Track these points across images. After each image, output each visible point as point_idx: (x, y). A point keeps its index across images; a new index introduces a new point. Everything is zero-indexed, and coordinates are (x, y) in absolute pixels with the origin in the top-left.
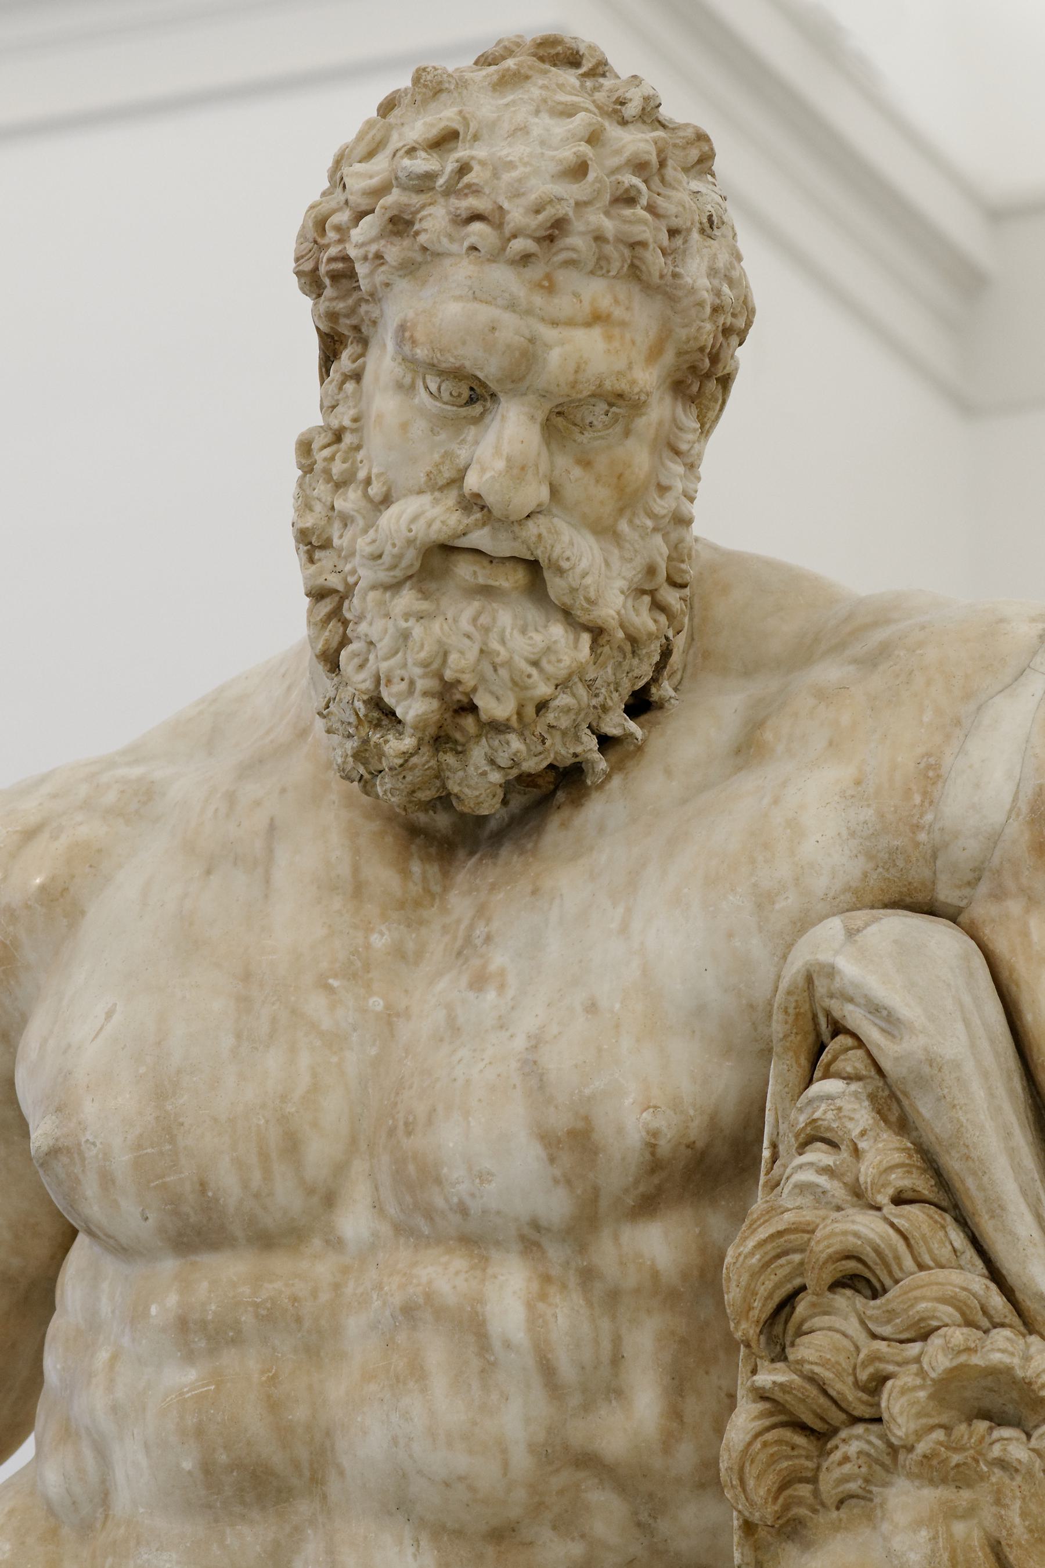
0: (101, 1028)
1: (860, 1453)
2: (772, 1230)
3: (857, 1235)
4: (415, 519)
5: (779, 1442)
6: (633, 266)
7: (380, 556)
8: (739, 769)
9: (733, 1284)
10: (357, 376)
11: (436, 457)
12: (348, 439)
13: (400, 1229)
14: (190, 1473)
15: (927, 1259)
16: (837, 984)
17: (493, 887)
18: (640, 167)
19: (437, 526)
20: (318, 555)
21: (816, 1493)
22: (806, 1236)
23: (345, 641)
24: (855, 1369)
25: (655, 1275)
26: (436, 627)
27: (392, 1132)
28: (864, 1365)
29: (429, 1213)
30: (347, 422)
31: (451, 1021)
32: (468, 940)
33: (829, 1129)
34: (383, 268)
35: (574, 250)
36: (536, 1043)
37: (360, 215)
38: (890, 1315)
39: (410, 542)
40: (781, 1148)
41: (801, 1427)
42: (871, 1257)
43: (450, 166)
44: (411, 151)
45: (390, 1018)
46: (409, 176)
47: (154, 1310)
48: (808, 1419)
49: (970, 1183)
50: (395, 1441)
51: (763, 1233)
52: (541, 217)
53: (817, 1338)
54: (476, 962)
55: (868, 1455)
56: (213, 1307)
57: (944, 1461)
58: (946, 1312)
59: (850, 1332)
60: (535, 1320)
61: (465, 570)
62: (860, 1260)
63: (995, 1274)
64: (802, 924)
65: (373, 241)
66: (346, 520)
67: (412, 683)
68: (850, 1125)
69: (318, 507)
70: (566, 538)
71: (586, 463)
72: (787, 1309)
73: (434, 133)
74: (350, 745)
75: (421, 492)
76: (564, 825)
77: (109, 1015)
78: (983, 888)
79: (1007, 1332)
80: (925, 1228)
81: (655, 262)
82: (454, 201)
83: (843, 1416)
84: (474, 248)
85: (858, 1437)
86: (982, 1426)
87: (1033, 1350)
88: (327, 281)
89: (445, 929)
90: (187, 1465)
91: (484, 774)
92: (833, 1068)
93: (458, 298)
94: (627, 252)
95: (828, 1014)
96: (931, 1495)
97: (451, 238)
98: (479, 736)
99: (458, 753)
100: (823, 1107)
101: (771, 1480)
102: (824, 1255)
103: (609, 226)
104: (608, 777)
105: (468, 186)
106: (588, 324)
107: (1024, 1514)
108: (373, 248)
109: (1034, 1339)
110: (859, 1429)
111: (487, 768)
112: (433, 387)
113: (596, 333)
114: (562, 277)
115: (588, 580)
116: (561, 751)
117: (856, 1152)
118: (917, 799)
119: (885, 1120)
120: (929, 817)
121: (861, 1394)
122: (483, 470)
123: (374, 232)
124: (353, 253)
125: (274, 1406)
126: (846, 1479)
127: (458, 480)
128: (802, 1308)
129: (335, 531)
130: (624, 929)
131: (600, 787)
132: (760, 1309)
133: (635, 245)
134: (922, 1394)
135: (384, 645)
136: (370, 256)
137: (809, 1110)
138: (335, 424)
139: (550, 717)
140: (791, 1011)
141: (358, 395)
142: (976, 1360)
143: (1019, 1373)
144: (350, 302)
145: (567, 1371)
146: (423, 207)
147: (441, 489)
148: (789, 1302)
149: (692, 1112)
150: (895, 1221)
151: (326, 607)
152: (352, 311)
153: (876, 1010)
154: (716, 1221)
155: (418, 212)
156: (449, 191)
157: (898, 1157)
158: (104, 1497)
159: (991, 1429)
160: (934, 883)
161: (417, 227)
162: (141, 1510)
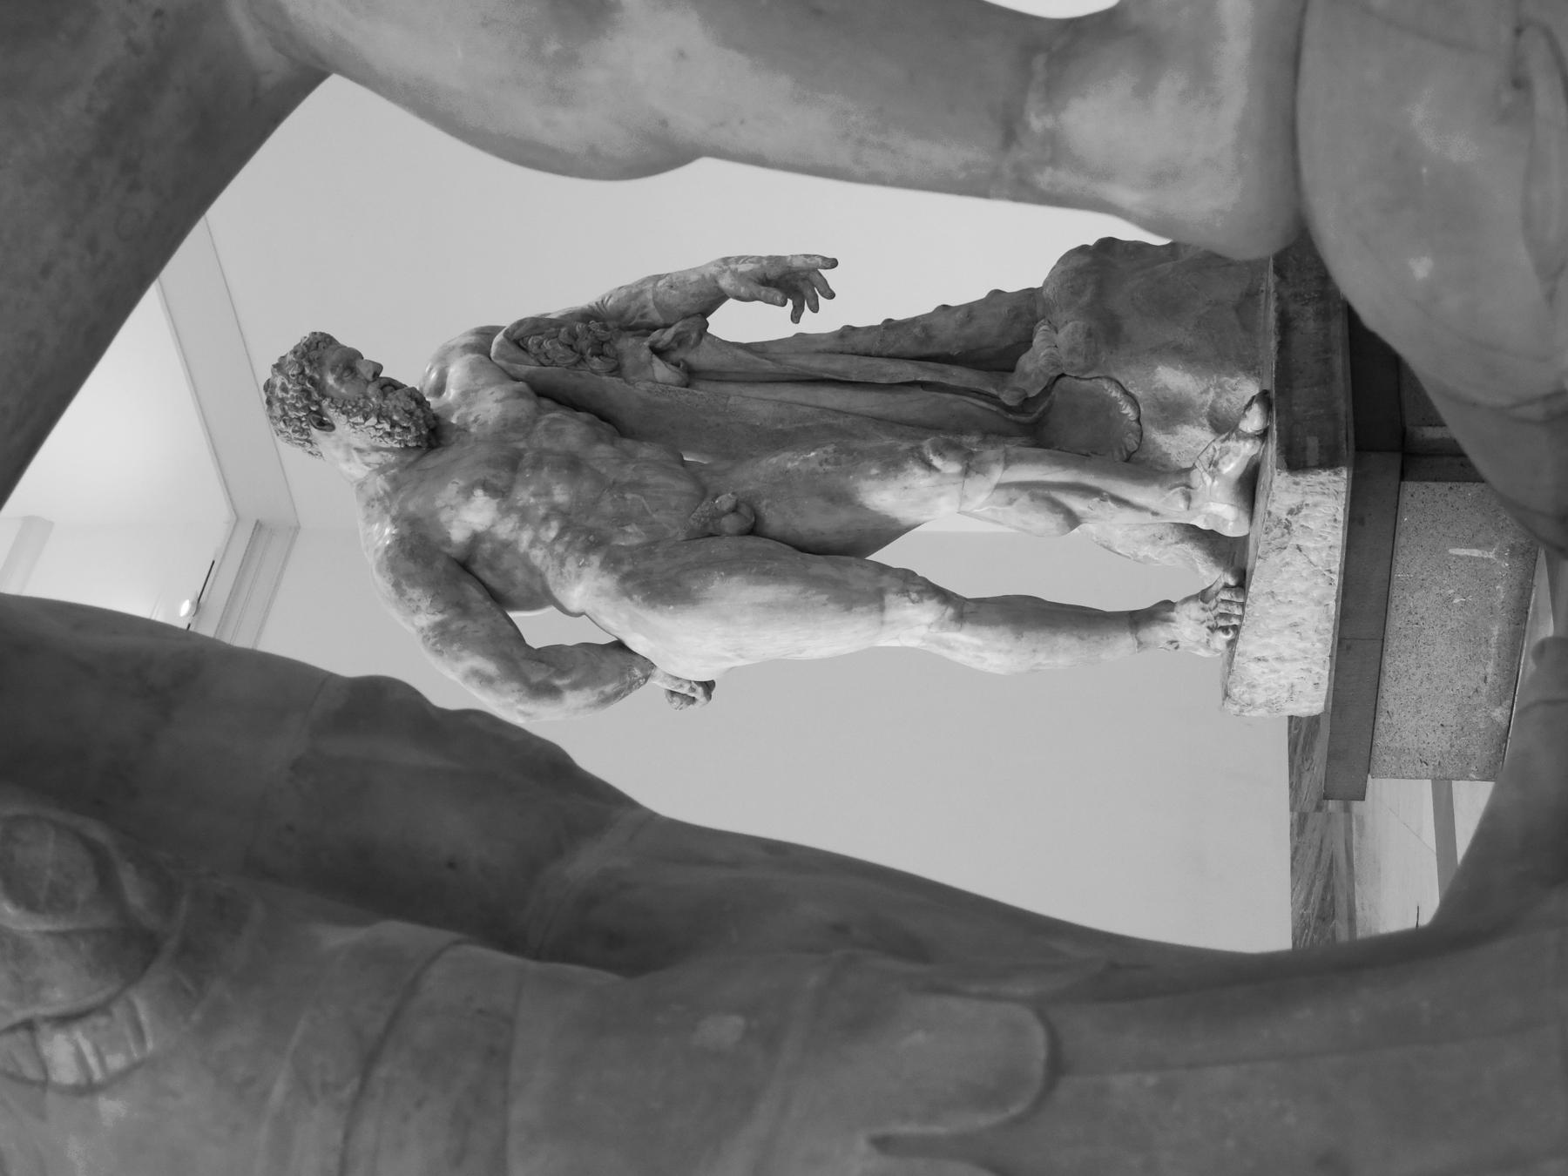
13: (527, 436)
16: (510, 331)
23: (391, 418)
36: (497, 401)
37: (302, 372)
45: (476, 440)
74: (413, 429)
82: (312, 348)
84: (324, 348)
90: (566, 472)
127: (368, 382)
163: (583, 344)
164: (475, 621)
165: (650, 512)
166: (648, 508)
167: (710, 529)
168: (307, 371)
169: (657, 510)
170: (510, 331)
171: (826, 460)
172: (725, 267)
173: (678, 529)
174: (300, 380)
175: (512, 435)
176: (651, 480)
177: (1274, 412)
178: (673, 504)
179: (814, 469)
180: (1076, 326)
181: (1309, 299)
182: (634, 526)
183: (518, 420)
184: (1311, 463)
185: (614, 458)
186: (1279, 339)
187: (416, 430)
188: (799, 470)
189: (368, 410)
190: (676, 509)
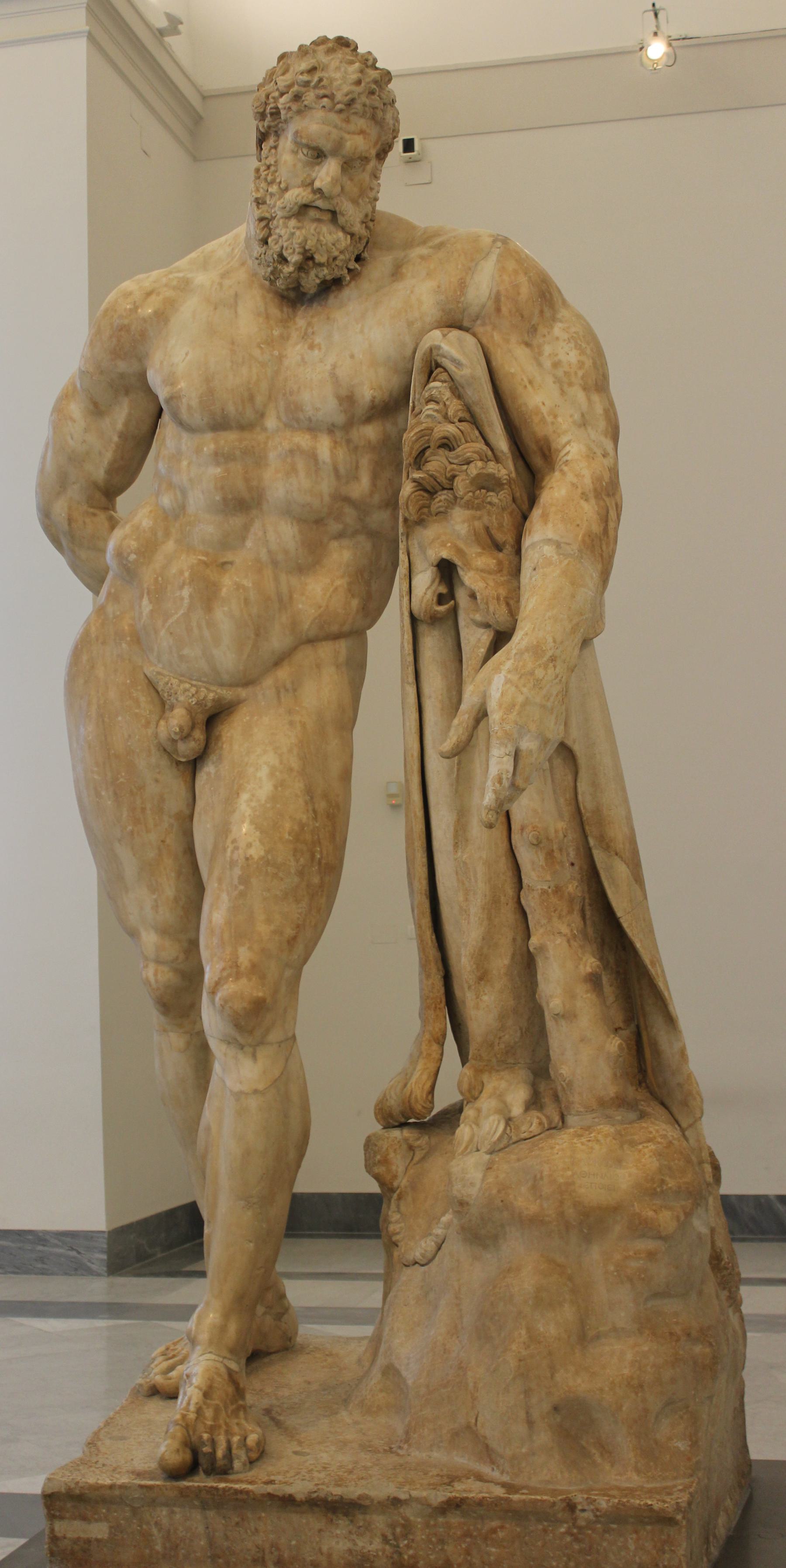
0: (185, 358)
1: (445, 499)
2: (419, 429)
3: (448, 431)
4: (298, 196)
5: (420, 495)
6: (373, 115)
7: (285, 208)
8: (394, 281)
9: (406, 446)
10: (275, 147)
11: (305, 175)
12: (272, 168)
13: (286, 425)
14: (218, 501)
15: (469, 439)
16: (441, 351)
17: (312, 317)
18: (376, 82)
19: (305, 198)
20: (260, 206)
21: (430, 512)
22: (430, 431)
23: (270, 235)
24: (445, 473)
25: (369, 442)
26: (304, 231)
27: (284, 395)
28: (449, 472)
29: (298, 420)
30: (272, 163)
31: (303, 359)
32: (306, 334)
33: (436, 397)
34: (291, 112)
35: (356, 109)
36: (334, 367)
37: (282, 95)
38: (458, 457)
39: (296, 203)
40: (416, 403)
41: (426, 490)
42: (452, 439)
43: (316, 79)
44: (302, 73)
45: (280, 358)
46: (302, 81)
47: (205, 449)
48: (429, 488)
49: (483, 416)
50: (287, 492)
51: (417, 430)
52: (348, 98)
53: (433, 463)
54: (310, 341)
55: (448, 500)
56: (226, 449)
57: (473, 502)
58: (476, 456)
59: (443, 462)
60: (333, 455)
61: (312, 213)
62: (449, 440)
63: (487, 443)
64: (423, 332)
65: (288, 103)
66: (272, 195)
67: (294, 250)
68: (443, 396)
69: (261, 191)
70: (345, 204)
71: (351, 180)
72: (421, 454)
73: (309, 67)
74: (269, 270)
75: (299, 187)
76: (336, 297)
77: (187, 354)
78: (479, 322)
79: (493, 463)
80: (469, 430)
81: (380, 114)
83: (441, 488)
84: (324, 107)
85: (445, 494)
86: (483, 491)
87: (500, 468)
88: (269, 116)
89: (297, 329)
90: (218, 498)
91: (314, 280)
92: (437, 378)
93: (317, 123)
94: (372, 110)
95: (436, 361)
96: (468, 513)
97: (316, 103)
98: (313, 268)
99: (305, 273)
100: (434, 391)
101: (417, 507)
102: (438, 438)
103: (368, 102)
104: (350, 282)
105: (323, 86)
106: (359, 134)
107: (496, 519)
108: (288, 105)
109: (500, 464)
110: (445, 492)
111: (315, 278)
112: (305, 152)
113: (361, 137)
114: (353, 118)
115: (351, 218)
116: (337, 273)
117: (445, 404)
118: (459, 293)
119: (454, 395)
120: (463, 299)
121: (447, 481)
122: (322, 181)
123: (288, 100)
124: (280, 106)
125: (247, 480)
126: (440, 507)
127: (312, 183)
128: (427, 453)
129: (268, 198)
130: (362, 332)
131: (347, 285)
132: (414, 454)
133: (375, 108)
134: (468, 481)
135: (285, 238)
136: (287, 107)
137: (430, 391)
138: (268, 163)
139: (337, 262)
140: (425, 359)
141: (276, 154)
142: (484, 471)
143: (497, 475)
144: (276, 123)
145: (342, 471)
146: (306, 92)
147: (307, 186)
148: (423, 451)
149: (385, 391)
150: (460, 427)
151: (263, 224)
152: (277, 126)
153: (453, 360)
154: (389, 426)
155: (304, 94)
156: (316, 87)
157: (460, 407)
158: (183, 507)
159: (486, 493)
160: (462, 320)
161: (303, 98)
162: (200, 512)
163: (437, 463)
164: (86, 430)
165: (167, 625)
166: (170, 621)
167: (167, 707)
168: (282, 100)
169: (171, 633)
170: (441, 351)
171: (236, 848)
172: (514, 652)
173: (160, 665)
174: (270, 97)
175: (282, 405)
176: (220, 614)
177: (143, 1482)
178: (186, 651)
179: (231, 832)
180: (472, 1184)
181: (398, 1547)
182: (150, 607)
183: (299, 408)
184: (60, 1527)
185: (269, 552)
186: (299, 1497)
187: (272, 273)
188: (234, 811)
189: (268, 202)
190: (181, 657)
